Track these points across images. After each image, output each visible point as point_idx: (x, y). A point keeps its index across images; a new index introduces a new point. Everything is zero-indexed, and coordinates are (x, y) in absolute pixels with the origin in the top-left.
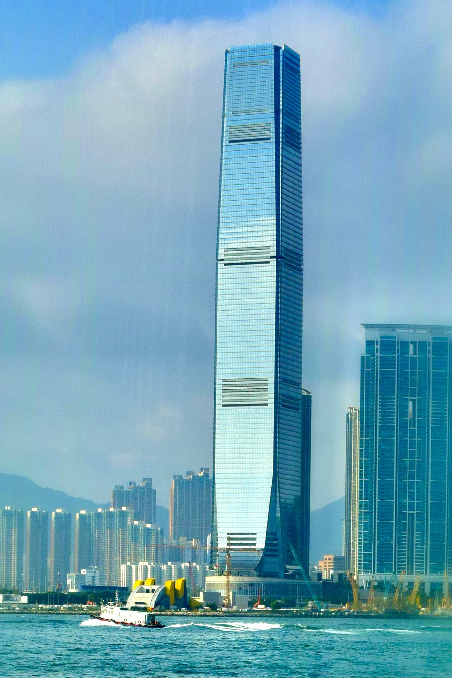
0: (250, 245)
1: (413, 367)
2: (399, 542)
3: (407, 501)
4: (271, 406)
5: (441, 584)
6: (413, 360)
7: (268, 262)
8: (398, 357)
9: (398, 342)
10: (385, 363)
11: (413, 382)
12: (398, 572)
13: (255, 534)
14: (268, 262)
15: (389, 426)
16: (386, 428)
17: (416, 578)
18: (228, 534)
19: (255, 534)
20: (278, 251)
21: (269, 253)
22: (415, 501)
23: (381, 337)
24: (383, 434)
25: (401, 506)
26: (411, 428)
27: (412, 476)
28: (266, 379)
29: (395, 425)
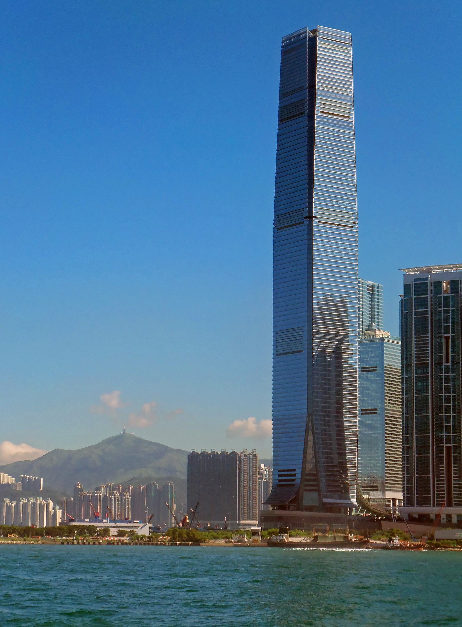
1: (446, 305)
2: (437, 475)
3: (444, 434)
6: (446, 298)
10: (422, 303)
12: (438, 505)
13: (294, 470)
15: (424, 363)
16: (422, 366)
18: (280, 471)
22: (452, 435)
24: (419, 371)
25: (439, 440)
26: (446, 364)
27: (447, 411)
29: (429, 362)
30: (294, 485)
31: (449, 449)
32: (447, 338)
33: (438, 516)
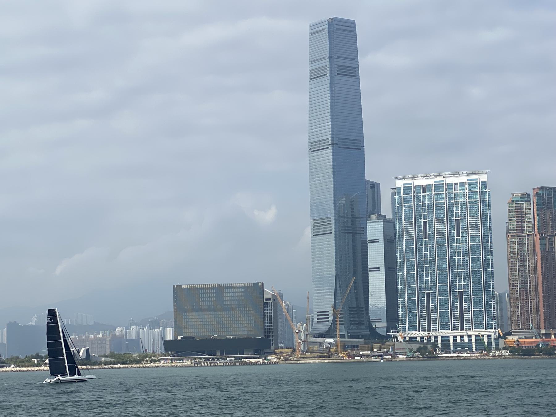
0: (321, 138)
4: (333, 233)
5: (448, 337)
7: (328, 148)
8: (414, 196)
9: (414, 186)
11: (424, 210)
13: (328, 312)
14: (328, 148)
17: (433, 333)
19: (328, 312)
20: (332, 140)
21: (328, 142)
23: (404, 184)
28: (330, 218)
30: (328, 321)
31: (428, 294)
32: (425, 223)
33: (422, 338)
